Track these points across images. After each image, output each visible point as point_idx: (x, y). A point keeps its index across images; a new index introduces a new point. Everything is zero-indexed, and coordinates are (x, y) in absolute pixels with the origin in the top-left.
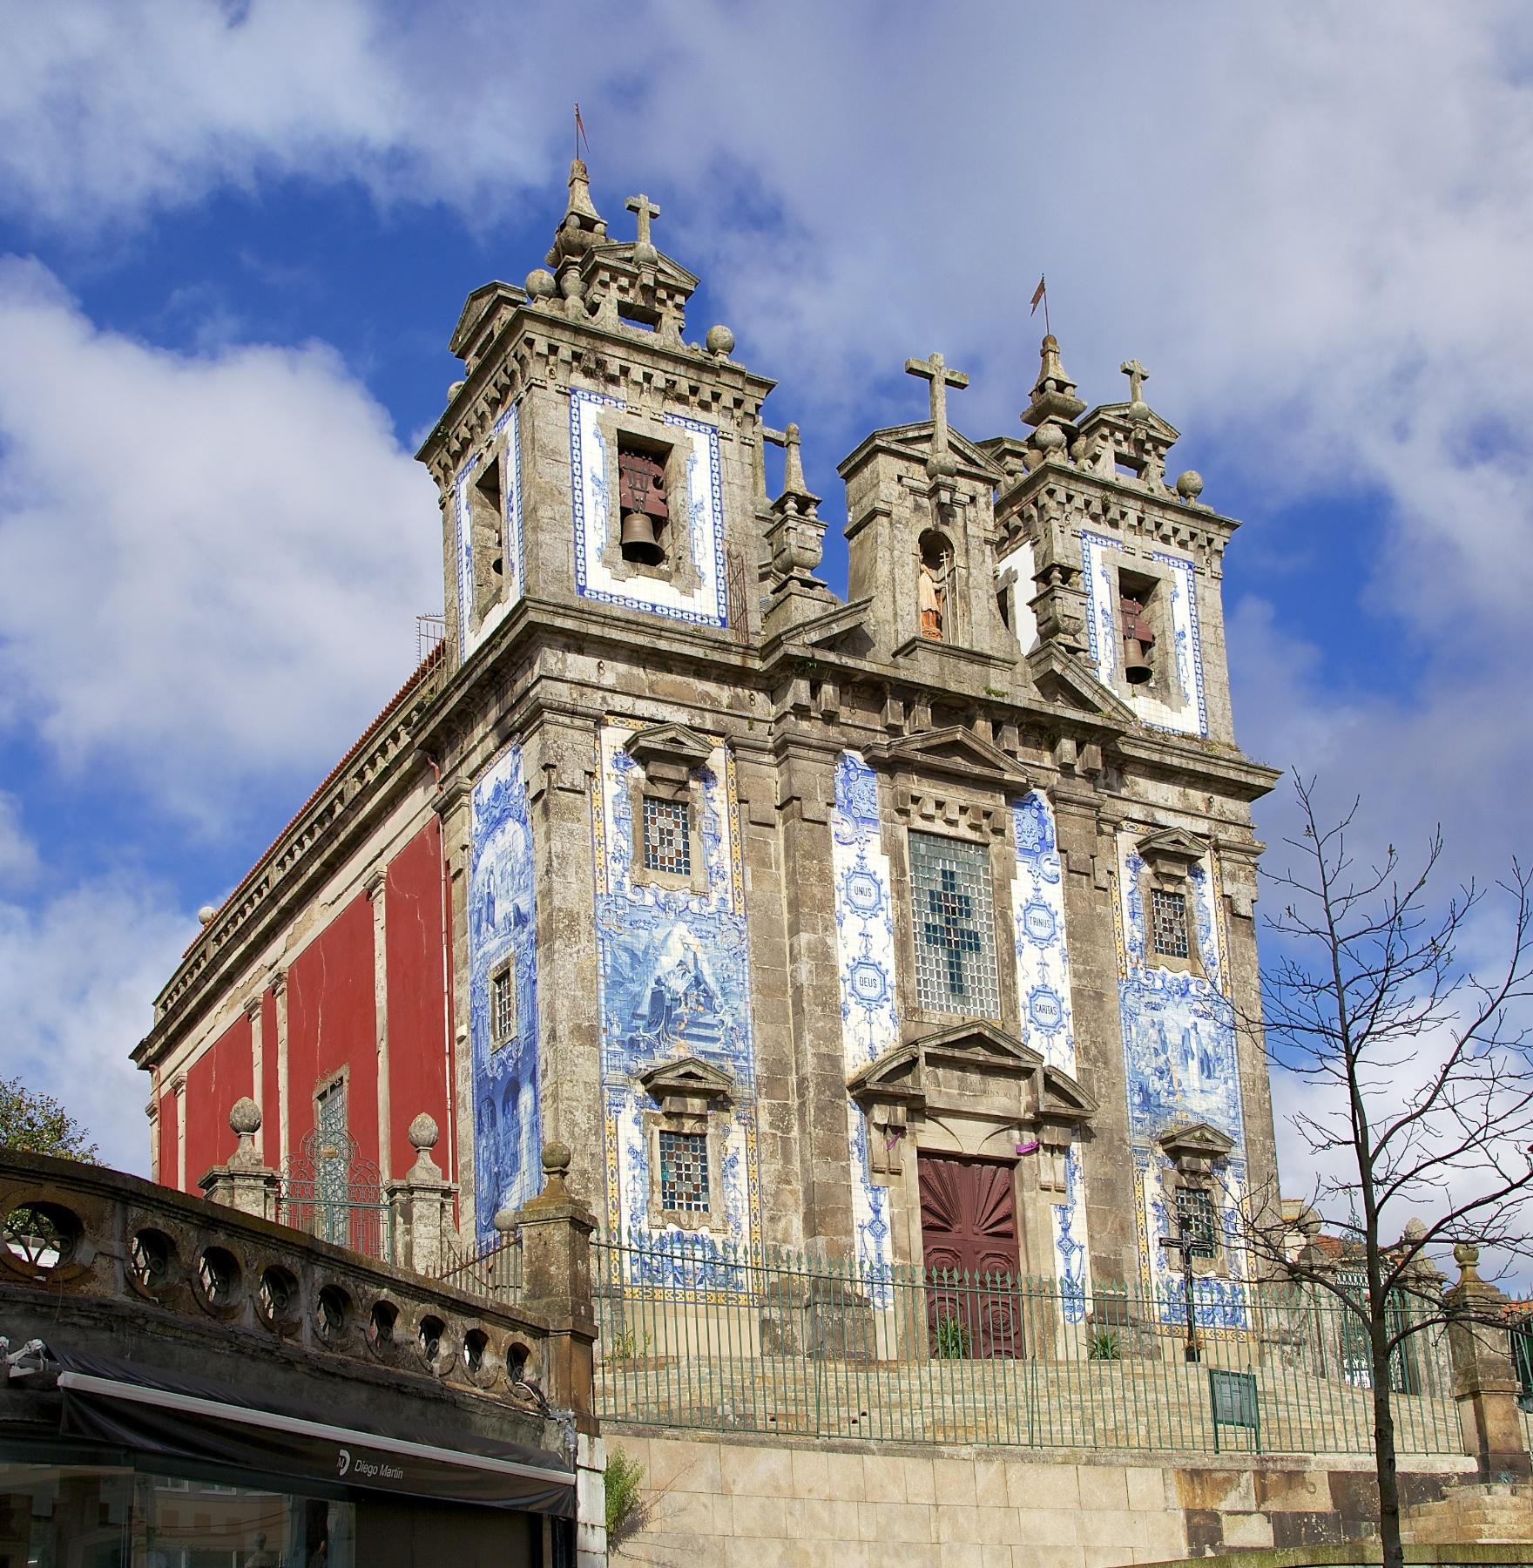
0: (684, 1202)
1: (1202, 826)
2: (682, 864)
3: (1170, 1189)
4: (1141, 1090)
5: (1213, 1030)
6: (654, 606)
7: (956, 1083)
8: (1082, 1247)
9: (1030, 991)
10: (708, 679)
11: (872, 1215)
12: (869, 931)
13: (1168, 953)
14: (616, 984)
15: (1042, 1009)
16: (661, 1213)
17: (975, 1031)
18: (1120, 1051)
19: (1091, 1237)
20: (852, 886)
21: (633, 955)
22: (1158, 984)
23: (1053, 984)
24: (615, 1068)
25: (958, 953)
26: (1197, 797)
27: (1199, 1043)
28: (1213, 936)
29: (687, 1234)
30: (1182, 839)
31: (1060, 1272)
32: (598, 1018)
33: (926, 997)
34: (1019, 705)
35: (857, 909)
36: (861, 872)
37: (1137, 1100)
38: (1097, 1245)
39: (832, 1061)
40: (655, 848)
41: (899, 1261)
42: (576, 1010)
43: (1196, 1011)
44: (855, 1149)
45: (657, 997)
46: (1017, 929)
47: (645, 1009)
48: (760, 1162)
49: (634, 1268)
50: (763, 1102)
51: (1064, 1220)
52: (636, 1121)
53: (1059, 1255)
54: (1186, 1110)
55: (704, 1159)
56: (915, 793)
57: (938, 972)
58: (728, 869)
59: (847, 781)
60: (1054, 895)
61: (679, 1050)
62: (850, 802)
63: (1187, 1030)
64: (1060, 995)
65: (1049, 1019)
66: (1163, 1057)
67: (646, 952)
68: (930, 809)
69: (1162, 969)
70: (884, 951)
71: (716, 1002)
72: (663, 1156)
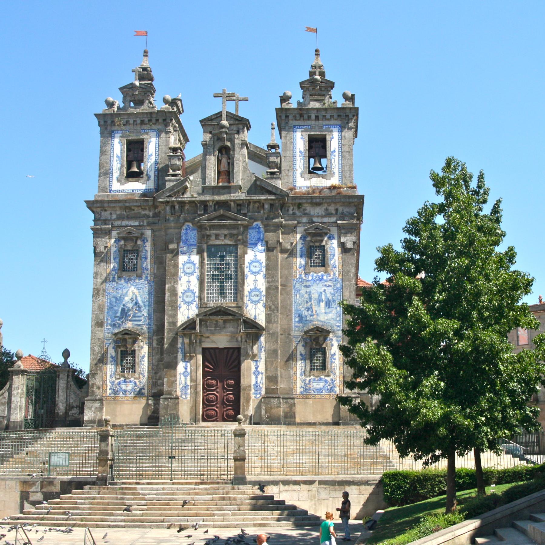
0: (128, 370)
1: (333, 219)
2: (135, 269)
3: (308, 349)
4: (299, 316)
5: (332, 291)
6: (133, 190)
7: (214, 326)
8: (262, 373)
9: (250, 290)
10: (146, 209)
11: (184, 370)
12: (190, 280)
13: (316, 266)
14: (111, 307)
15: (254, 296)
16: (119, 374)
17: (218, 309)
18: (291, 304)
19: (266, 369)
20: (185, 267)
21: (116, 298)
22: (310, 278)
23: (258, 287)
24: (108, 333)
25: (223, 282)
26: (332, 209)
27: (326, 296)
28: (336, 257)
29: (128, 380)
30: (319, 227)
31: (253, 382)
32: (104, 319)
33: (210, 297)
34: (242, 198)
35: (186, 274)
36: (189, 262)
37: (297, 320)
38: (268, 372)
39: (174, 323)
40: (127, 265)
41: (193, 384)
42: (97, 317)
43: (325, 285)
44: (180, 350)
45: (123, 310)
46: (246, 271)
47: (119, 314)
48: (153, 356)
49: (110, 391)
50: (155, 337)
51: (257, 364)
52: (113, 348)
53: (253, 377)
54: (318, 321)
55: (135, 357)
56: (208, 234)
57: (216, 290)
58: (149, 267)
59: (186, 234)
60: (262, 257)
61: (129, 325)
62: (187, 240)
63: (321, 293)
64: (261, 290)
65: (256, 299)
66: (310, 303)
67: (120, 297)
68: (213, 238)
69: (312, 273)
70: (195, 286)
71: (142, 309)
72: (121, 357)
